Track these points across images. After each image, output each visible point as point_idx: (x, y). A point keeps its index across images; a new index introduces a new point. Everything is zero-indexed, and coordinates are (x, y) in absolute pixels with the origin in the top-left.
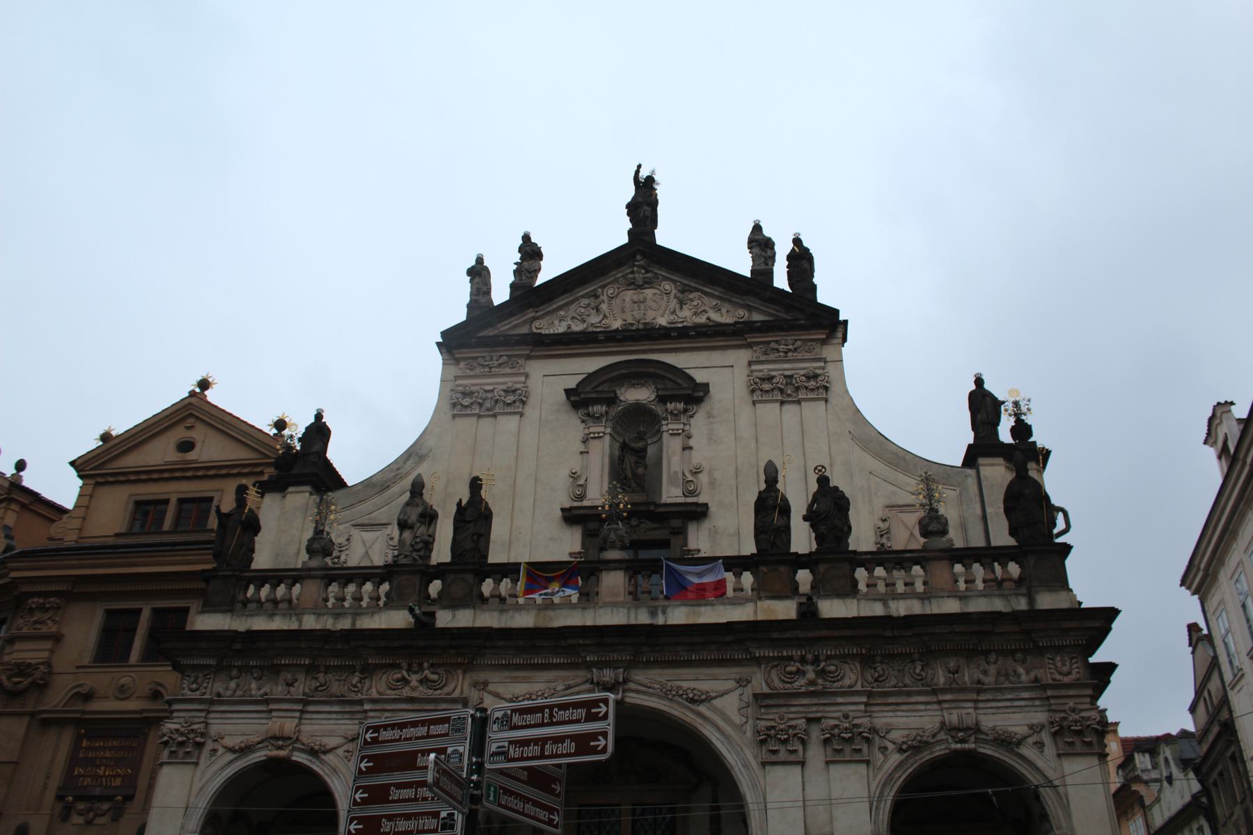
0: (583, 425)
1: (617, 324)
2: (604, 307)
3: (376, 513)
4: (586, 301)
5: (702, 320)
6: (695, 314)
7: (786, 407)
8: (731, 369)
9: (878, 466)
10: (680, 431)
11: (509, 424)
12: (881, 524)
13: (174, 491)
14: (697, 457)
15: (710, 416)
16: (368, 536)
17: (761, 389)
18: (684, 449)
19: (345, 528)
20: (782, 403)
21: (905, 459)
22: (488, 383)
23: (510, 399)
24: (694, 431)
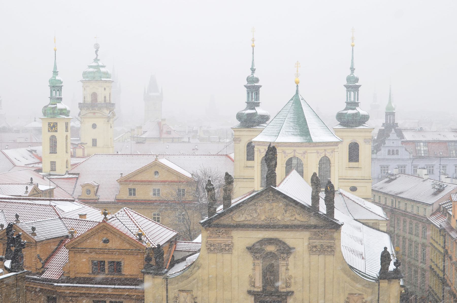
0: (252, 259)
1: (263, 218)
2: (258, 211)
3: (186, 287)
4: (251, 208)
5: (293, 219)
6: (291, 216)
7: (320, 256)
8: (303, 239)
9: (348, 279)
10: (285, 264)
11: (227, 256)
12: (347, 300)
13: (107, 258)
14: (290, 273)
15: (295, 257)
16: (185, 294)
17: (313, 249)
18: (286, 270)
19: (176, 291)
20: (319, 255)
21: (357, 278)
22: (219, 240)
23: (227, 248)
24: (290, 263)
